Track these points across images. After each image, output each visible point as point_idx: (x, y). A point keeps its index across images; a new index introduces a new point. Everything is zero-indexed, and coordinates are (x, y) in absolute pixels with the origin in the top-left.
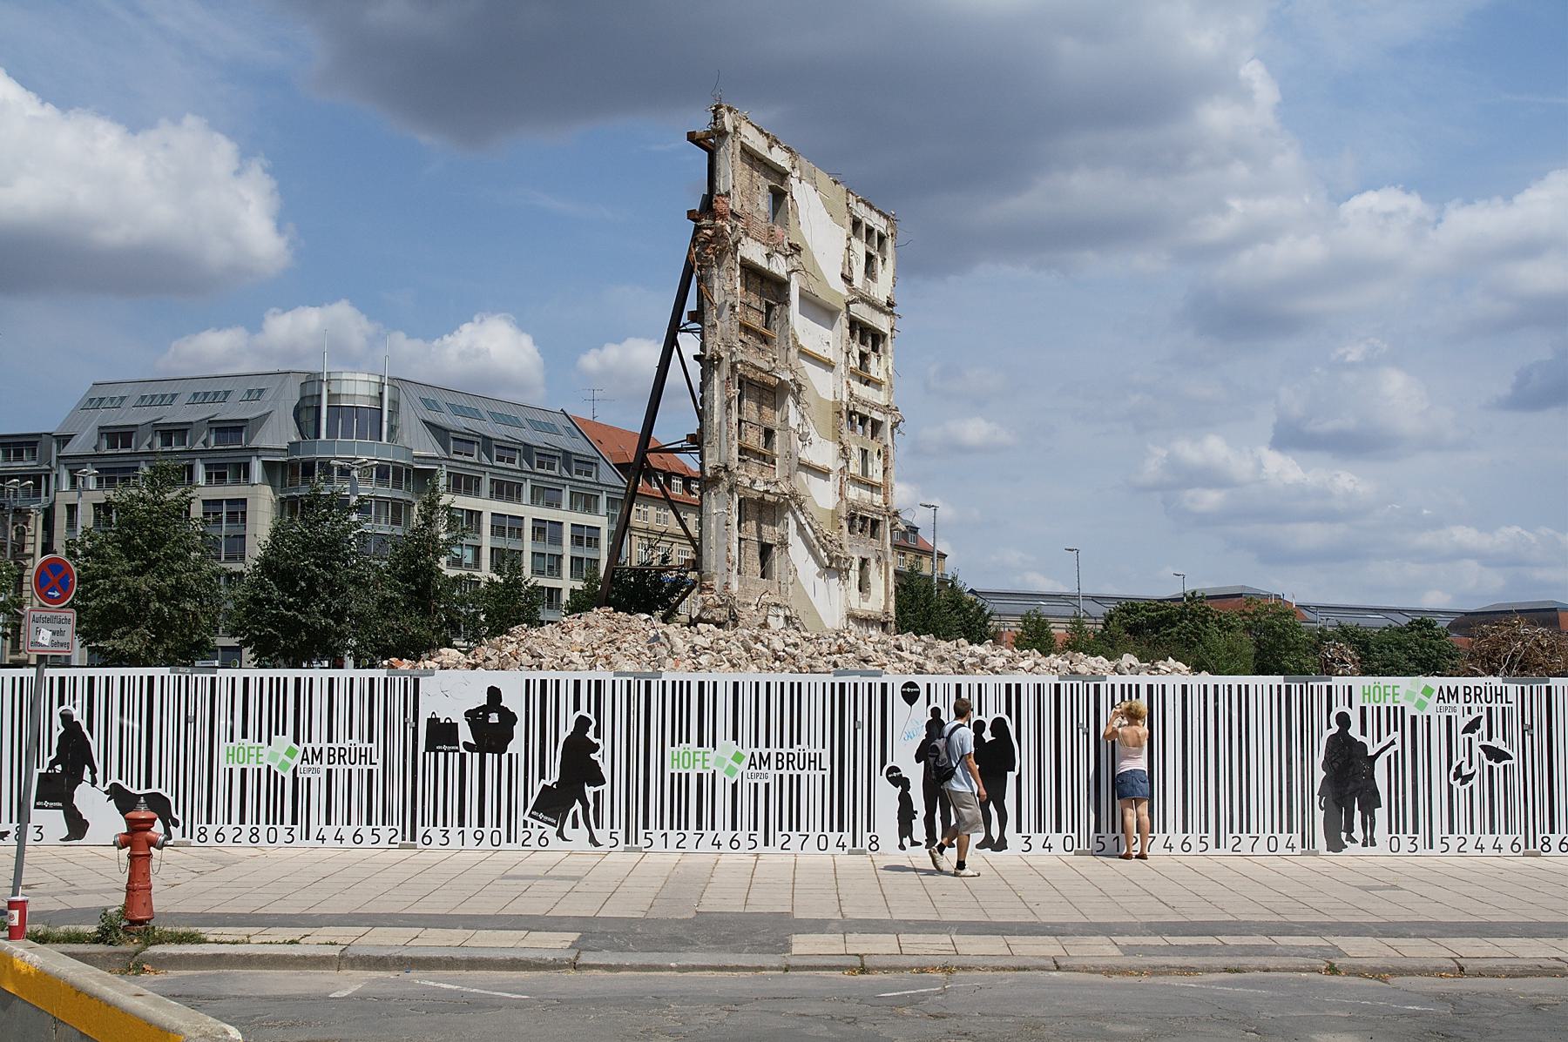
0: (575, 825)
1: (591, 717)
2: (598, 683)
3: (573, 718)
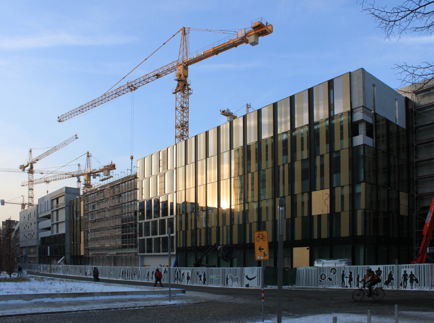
0: (390, 286)
1: (392, 271)
2: (393, 266)
3: (390, 271)
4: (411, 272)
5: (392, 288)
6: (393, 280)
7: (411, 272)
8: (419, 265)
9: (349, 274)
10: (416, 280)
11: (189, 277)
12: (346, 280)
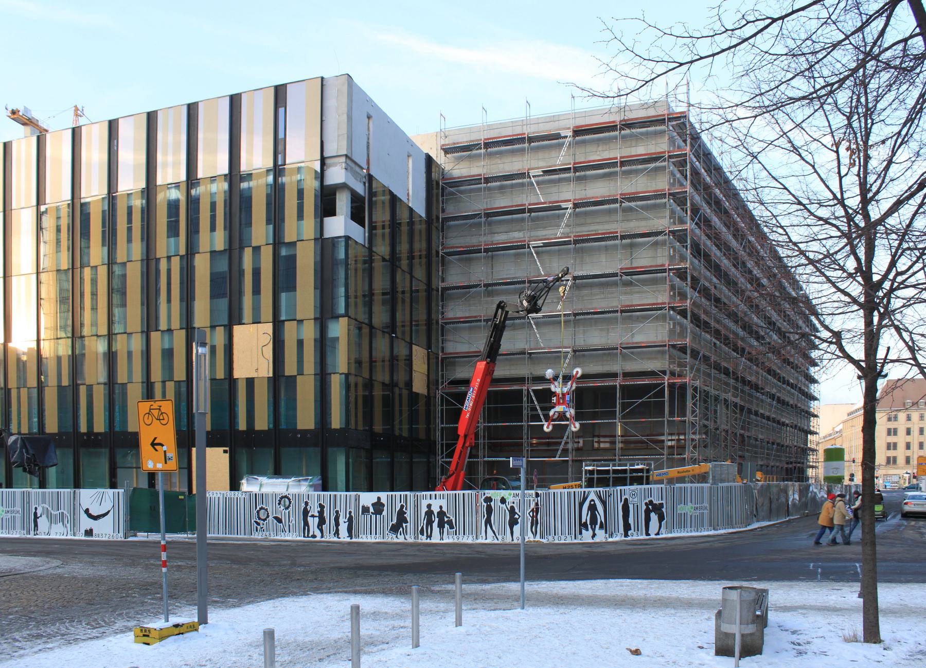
4: (441, 507)
7: (441, 507)
9: (319, 509)
10: (450, 523)
12: (313, 522)
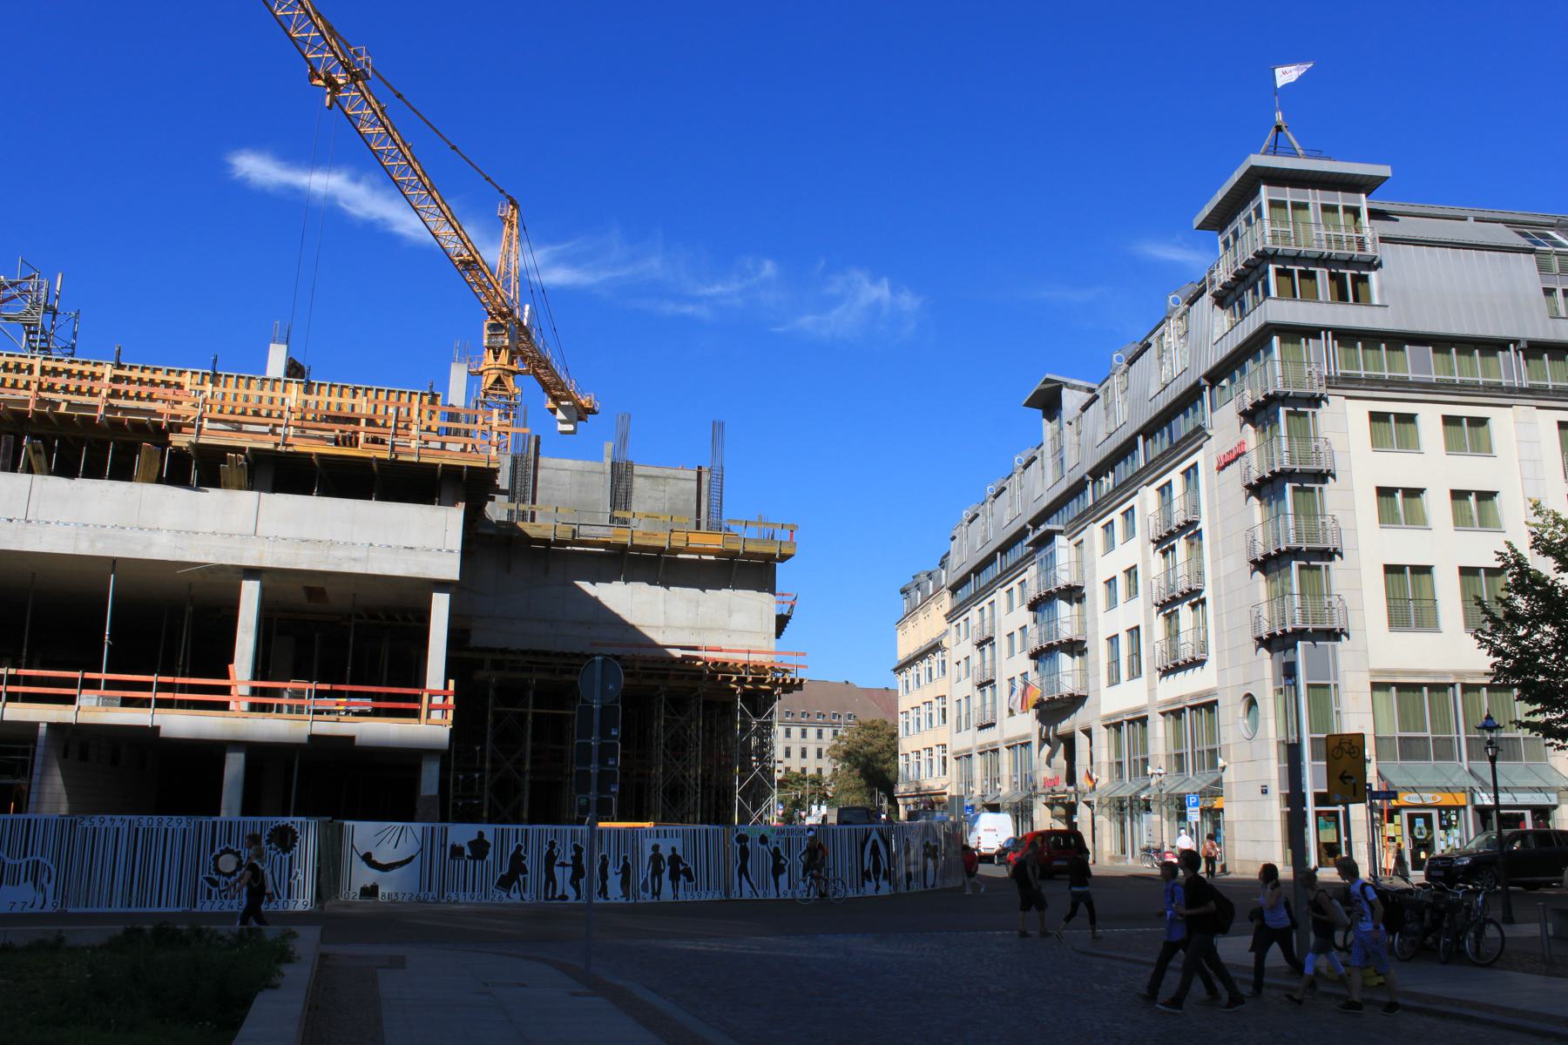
0: (515, 892)
4: (674, 850)
5: (522, 898)
6: (525, 872)
7: (674, 850)
8: (503, 830)
9: (574, 853)
11: (629, 864)
12: (563, 875)
